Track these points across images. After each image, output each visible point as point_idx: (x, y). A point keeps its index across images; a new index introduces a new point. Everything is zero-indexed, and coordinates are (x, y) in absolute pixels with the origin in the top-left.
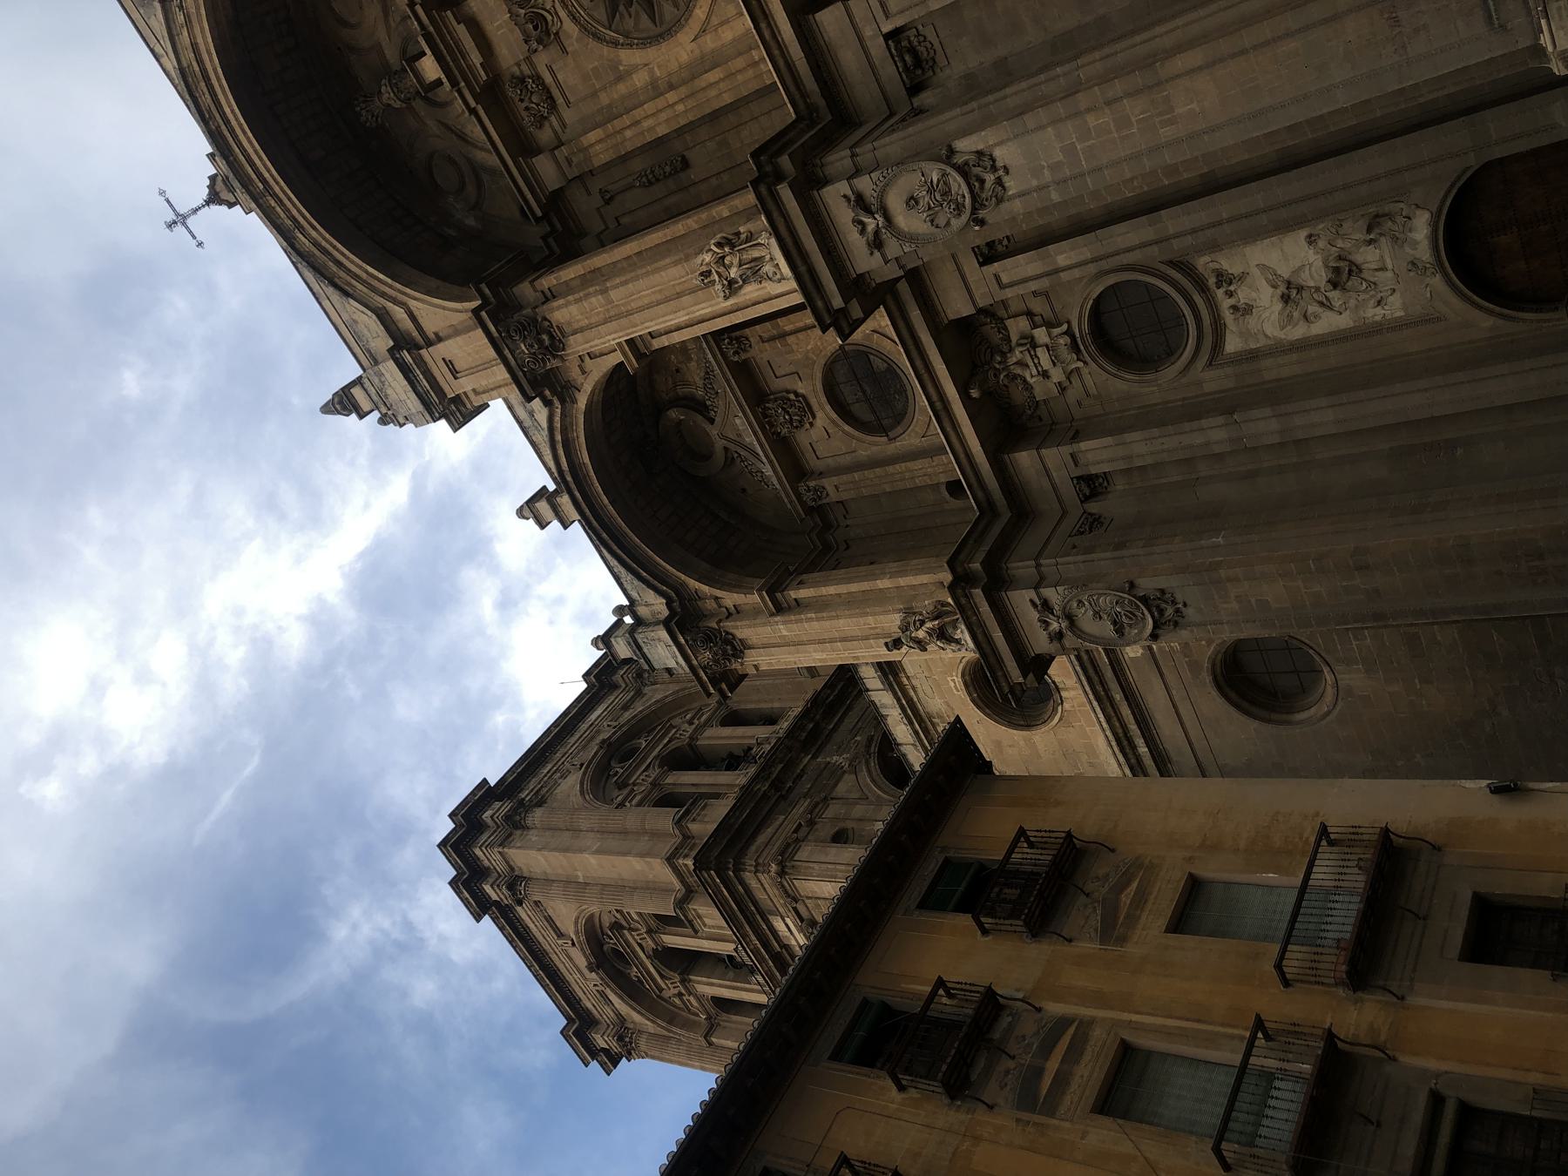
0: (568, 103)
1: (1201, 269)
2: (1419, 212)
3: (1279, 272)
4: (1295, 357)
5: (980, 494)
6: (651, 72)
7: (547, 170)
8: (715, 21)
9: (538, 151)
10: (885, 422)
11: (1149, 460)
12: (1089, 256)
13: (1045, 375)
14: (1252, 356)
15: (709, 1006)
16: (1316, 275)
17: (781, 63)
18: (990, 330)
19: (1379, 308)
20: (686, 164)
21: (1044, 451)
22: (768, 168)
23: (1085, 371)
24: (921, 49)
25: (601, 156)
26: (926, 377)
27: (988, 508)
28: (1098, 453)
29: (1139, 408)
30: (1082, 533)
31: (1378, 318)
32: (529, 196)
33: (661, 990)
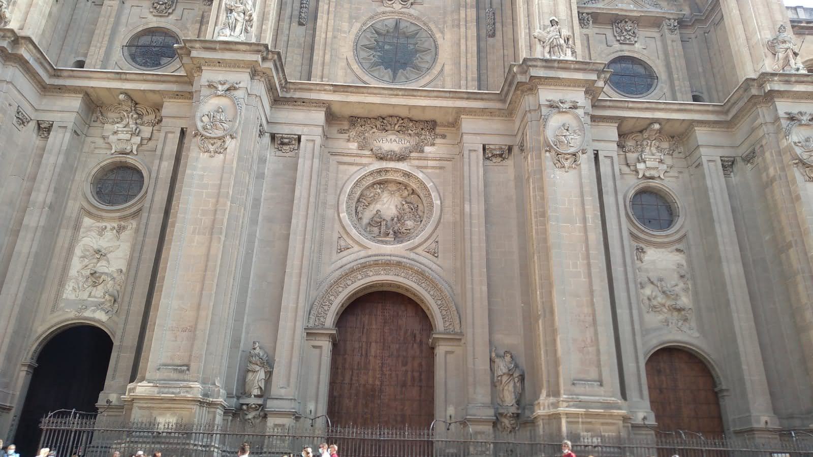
1: (132, 221)
2: (107, 317)
3: (111, 253)
4: (66, 245)
5: (65, 74)
6: (345, 33)
8: (349, 71)
10: (134, 49)
11: (44, 161)
12: (160, 176)
13: (115, 133)
14: (77, 227)
16: (102, 267)
17: (312, 87)
18: (151, 117)
19: (71, 288)
20: (300, 24)
21: (75, 114)
22: (270, 56)
23: (109, 152)
24: (287, 147)
26: (141, 77)
27: (56, 73)
28: (59, 139)
29: (77, 168)
30: (18, 113)
31: (67, 287)
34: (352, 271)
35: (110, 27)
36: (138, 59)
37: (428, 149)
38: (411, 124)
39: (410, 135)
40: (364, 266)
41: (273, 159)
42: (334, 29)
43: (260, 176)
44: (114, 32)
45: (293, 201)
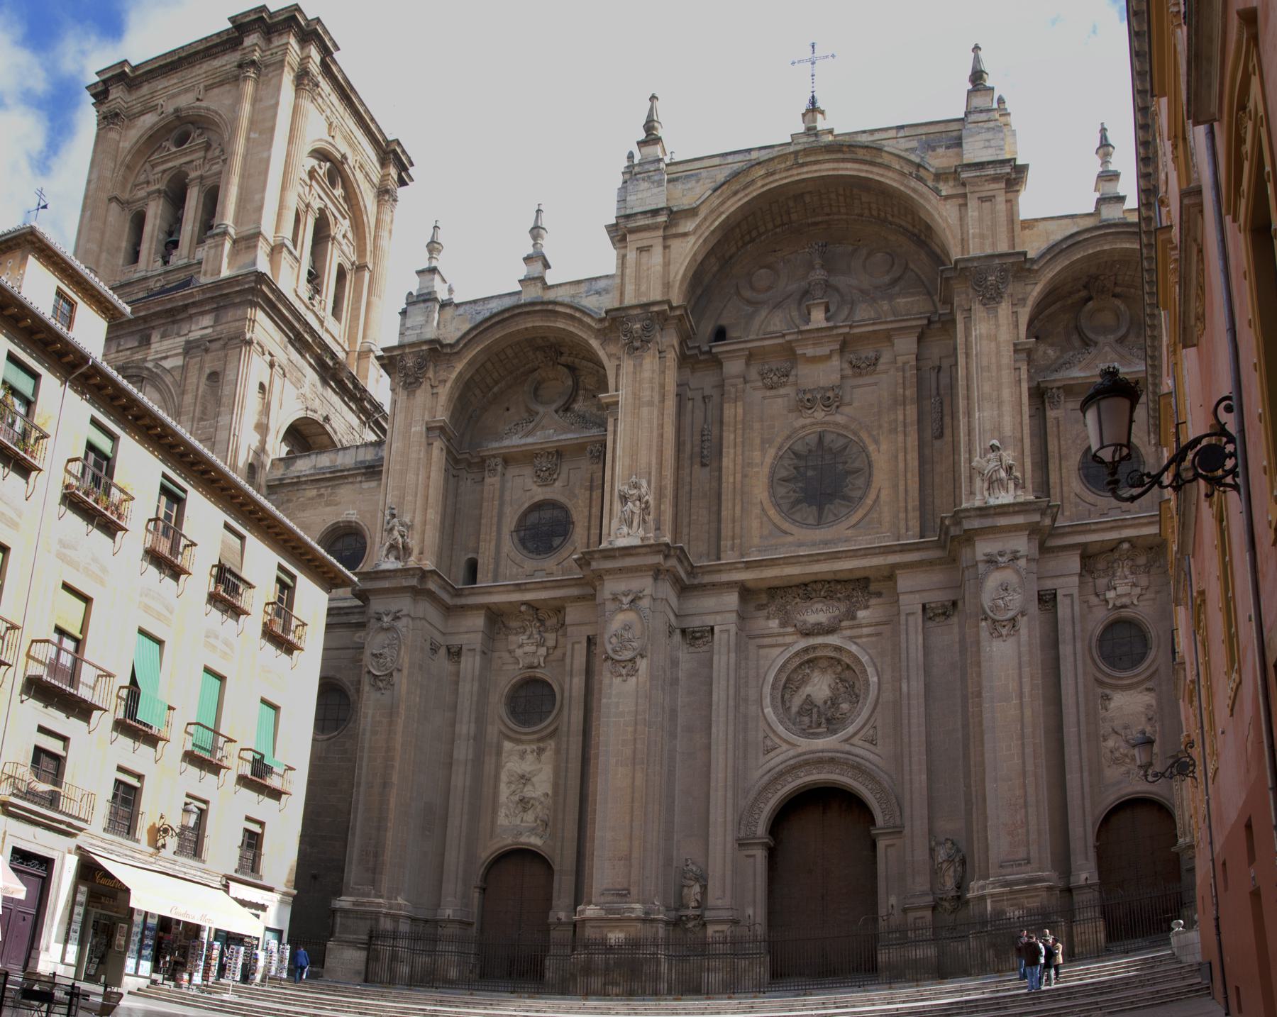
0: (764, 398)
5: (467, 592)
7: (734, 367)
9: (748, 364)
10: (522, 533)
11: (460, 690)
13: (521, 646)
15: (137, 207)
18: (554, 620)
21: (481, 634)
24: (700, 641)
25: (729, 411)
26: (540, 586)
27: (458, 593)
28: (470, 664)
32: (725, 349)
33: (153, 167)
34: (781, 774)
35: (495, 512)
36: (529, 545)
37: (861, 614)
38: (839, 587)
39: (839, 599)
40: (794, 768)
41: (686, 657)
42: (743, 467)
43: (675, 682)
44: (500, 515)
45: (710, 705)
